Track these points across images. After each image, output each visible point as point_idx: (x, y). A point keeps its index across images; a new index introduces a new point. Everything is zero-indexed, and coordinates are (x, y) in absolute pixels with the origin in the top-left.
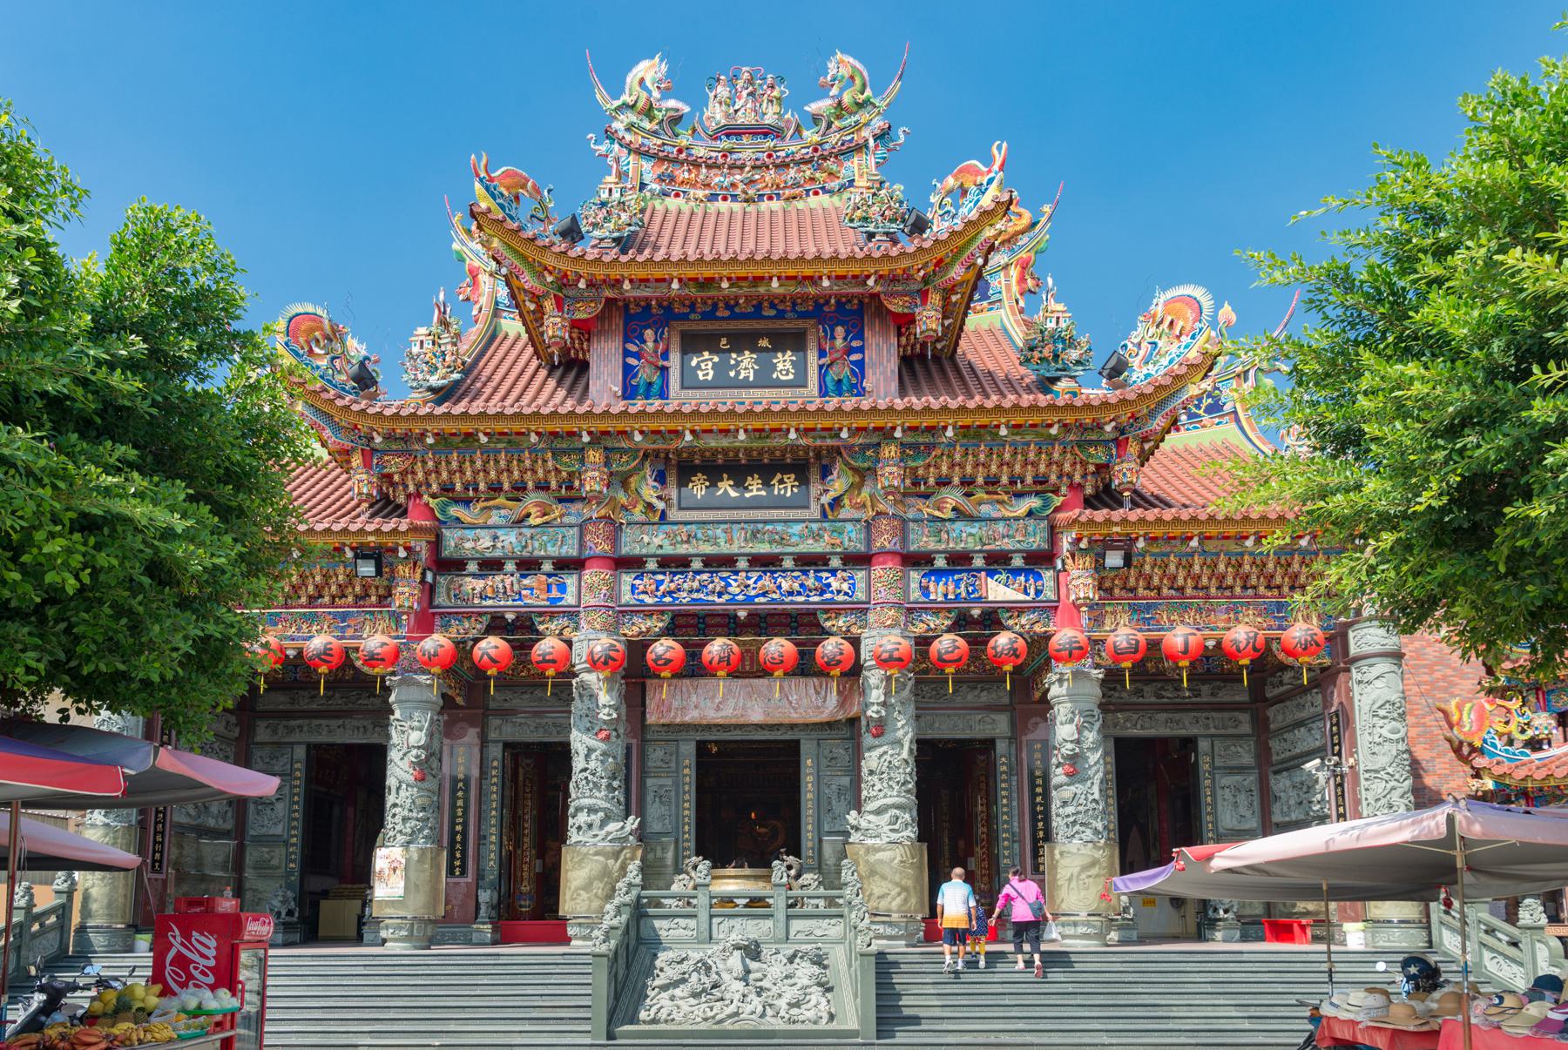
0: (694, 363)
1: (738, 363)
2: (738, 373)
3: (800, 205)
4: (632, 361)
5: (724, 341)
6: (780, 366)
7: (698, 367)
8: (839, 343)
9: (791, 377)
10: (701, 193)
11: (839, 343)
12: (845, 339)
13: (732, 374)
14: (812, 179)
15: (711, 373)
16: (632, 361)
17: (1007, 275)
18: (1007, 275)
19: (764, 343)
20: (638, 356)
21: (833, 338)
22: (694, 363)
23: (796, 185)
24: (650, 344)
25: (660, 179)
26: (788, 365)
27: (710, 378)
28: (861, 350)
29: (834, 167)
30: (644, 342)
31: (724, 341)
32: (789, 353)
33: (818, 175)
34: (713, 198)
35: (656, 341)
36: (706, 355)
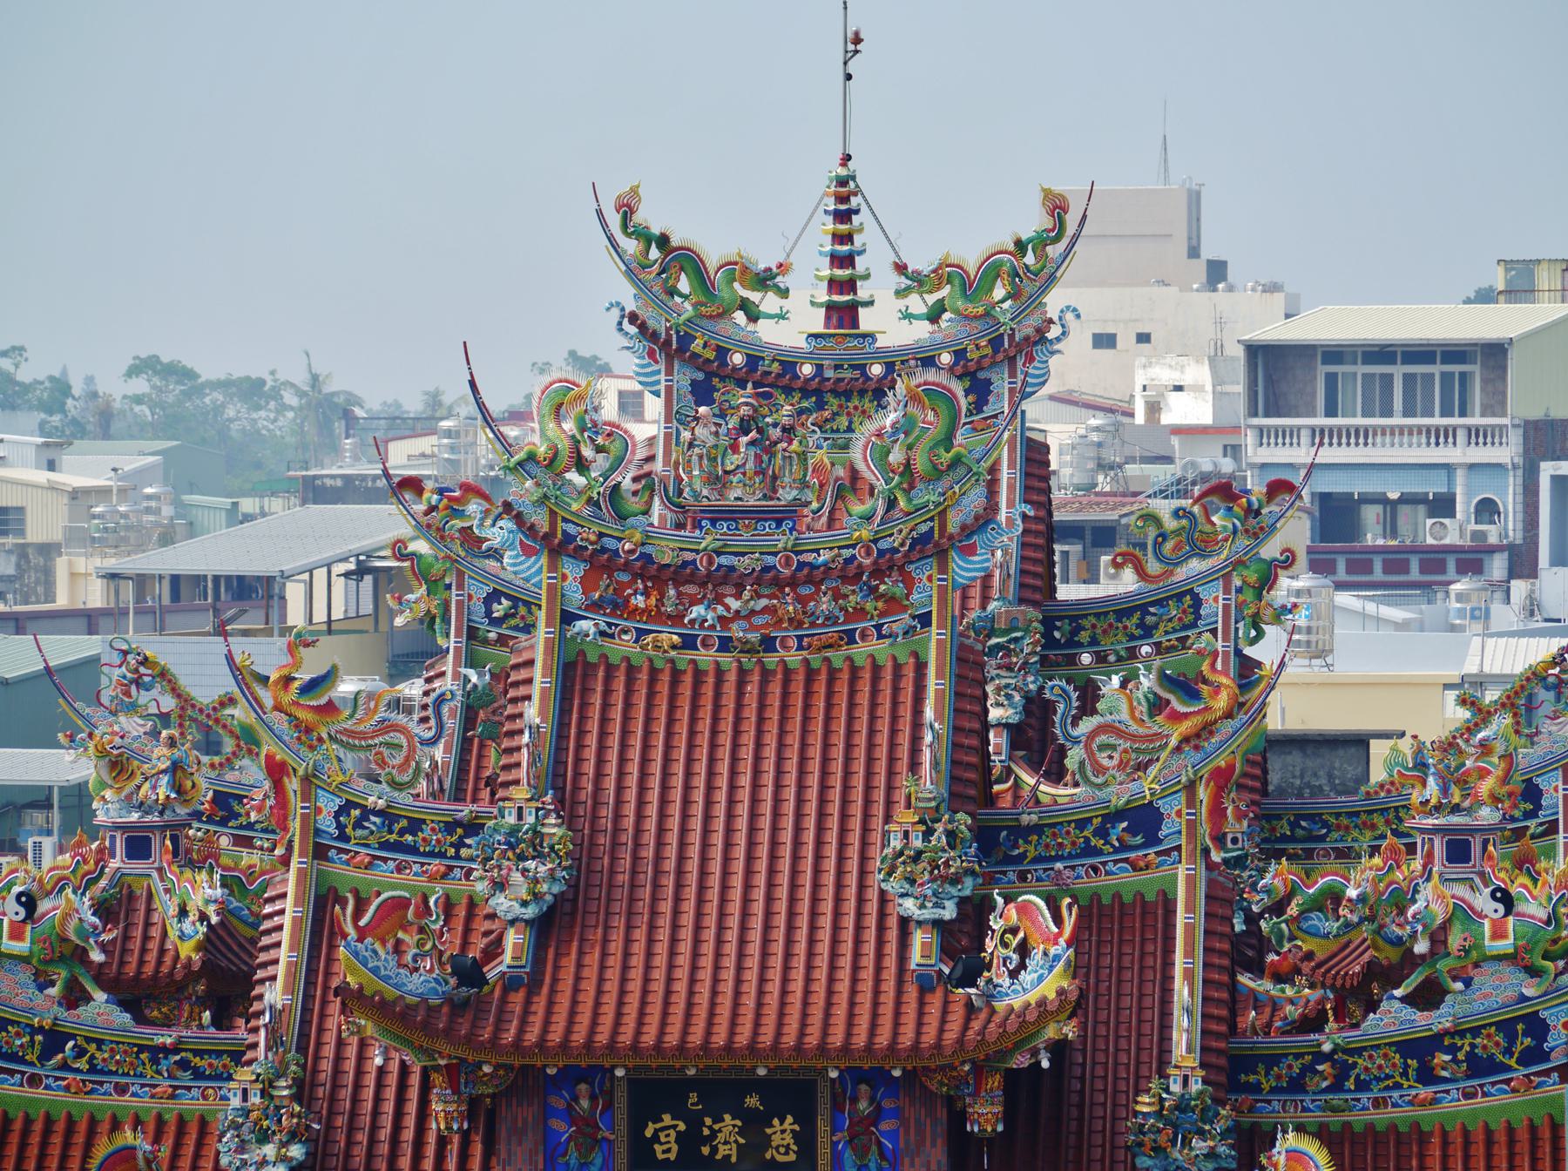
0: (649, 1133)
1: (714, 1134)
2: (715, 1150)
3: (837, 658)
4: (557, 1124)
5: (693, 1098)
6: (776, 1140)
7: (655, 1138)
8: (863, 1105)
9: (792, 1157)
10: (669, 636)
11: (863, 1105)
12: (872, 1100)
13: (706, 1150)
14: (860, 613)
15: (675, 1148)
16: (557, 1124)
17: (1191, 801)
18: (1191, 801)
19: (752, 1101)
20: (570, 1116)
21: (854, 1100)
22: (649, 1133)
23: (830, 619)
24: (585, 1103)
25: (595, 607)
26: (789, 1139)
27: (672, 1156)
28: (896, 1113)
29: (900, 590)
30: (576, 1099)
31: (693, 1098)
32: (790, 1119)
33: (869, 606)
34: (688, 643)
35: (593, 1098)
36: (667, 1119)
